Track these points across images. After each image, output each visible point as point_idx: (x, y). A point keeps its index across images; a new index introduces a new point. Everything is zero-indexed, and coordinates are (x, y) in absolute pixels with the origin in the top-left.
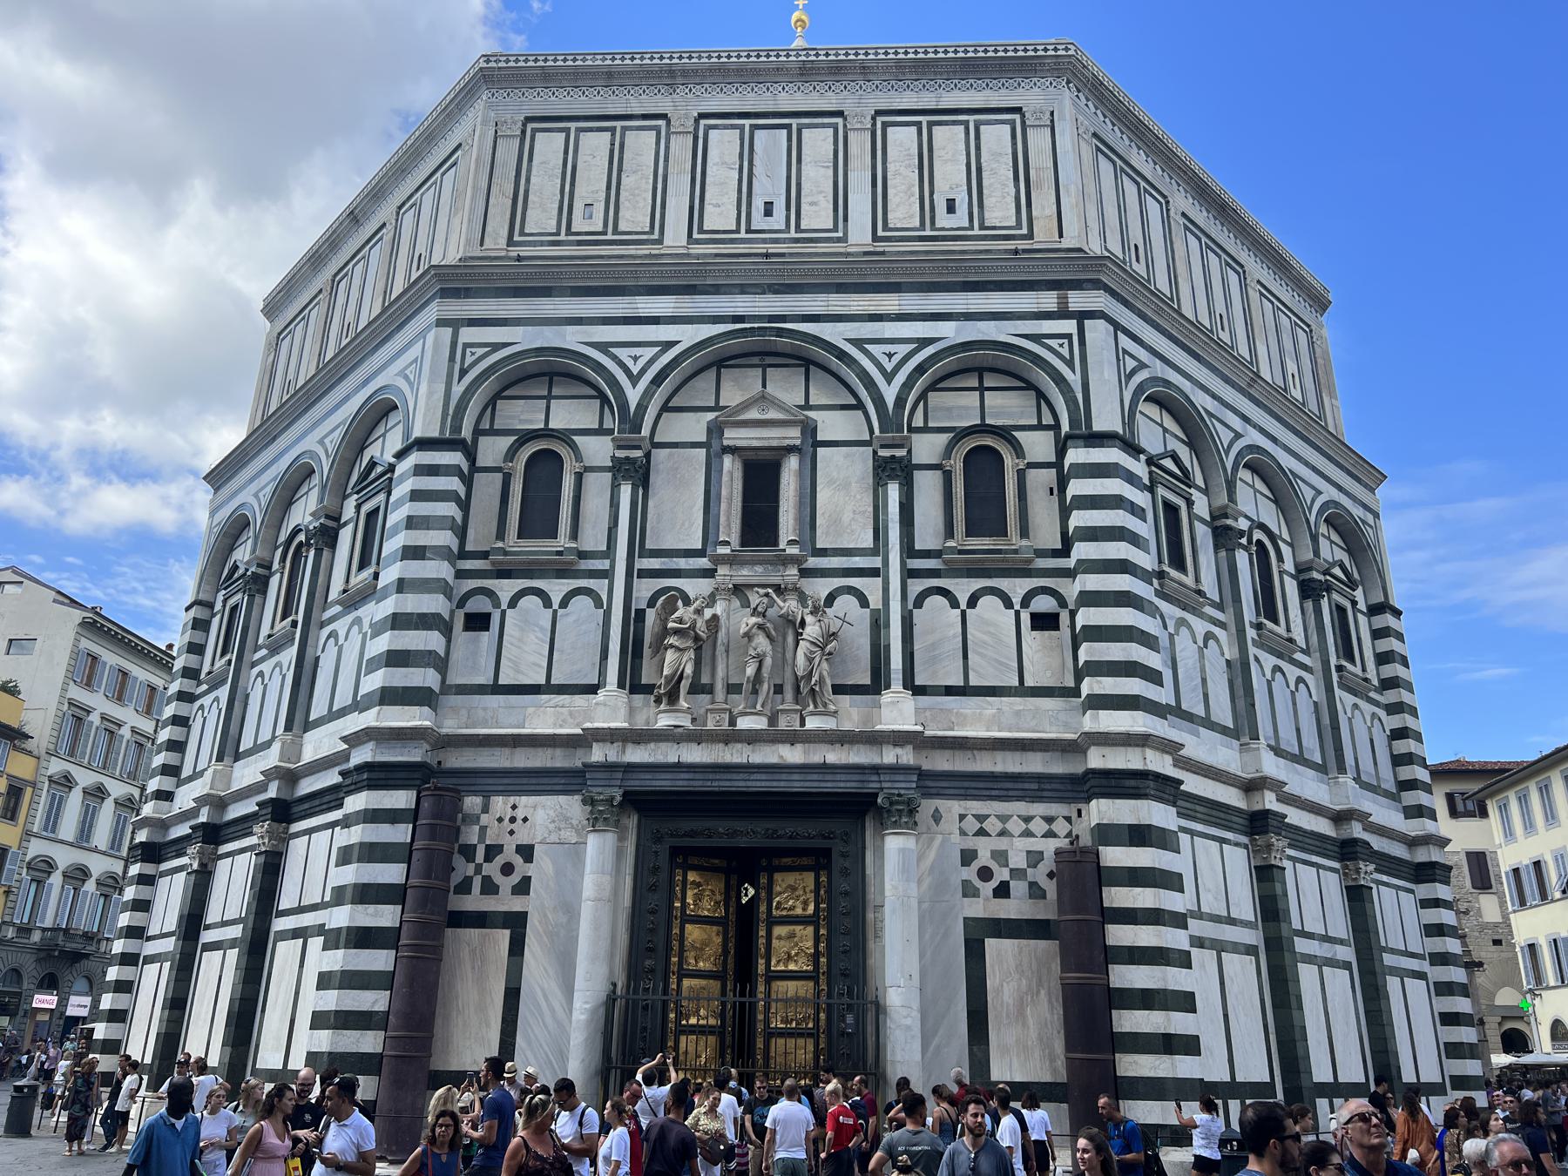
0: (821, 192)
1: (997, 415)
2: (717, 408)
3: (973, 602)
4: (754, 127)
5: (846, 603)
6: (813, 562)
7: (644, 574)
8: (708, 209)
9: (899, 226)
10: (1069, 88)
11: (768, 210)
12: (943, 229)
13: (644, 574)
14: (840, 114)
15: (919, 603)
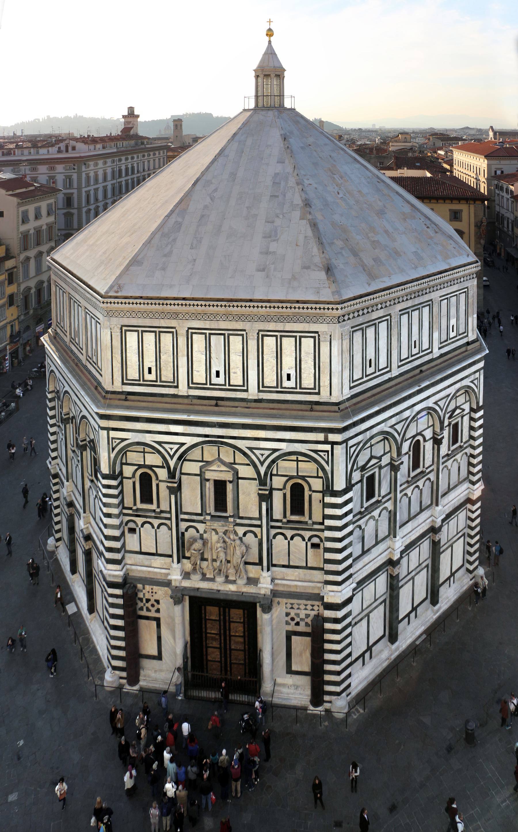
0: (238, 368)
1: (302, 472)
2: (202, 461)
3: (292, 538)
4: (210, 334)
5: (250, 536)
6: (238, 521)
7: (183, 520)
8: (195, 373)
9: (268, 385)
10: (339, 322)
11: (218, 374)
12: (285, 388)
13: (183, 520)
14: (245, 330)
15: (274, 537)
